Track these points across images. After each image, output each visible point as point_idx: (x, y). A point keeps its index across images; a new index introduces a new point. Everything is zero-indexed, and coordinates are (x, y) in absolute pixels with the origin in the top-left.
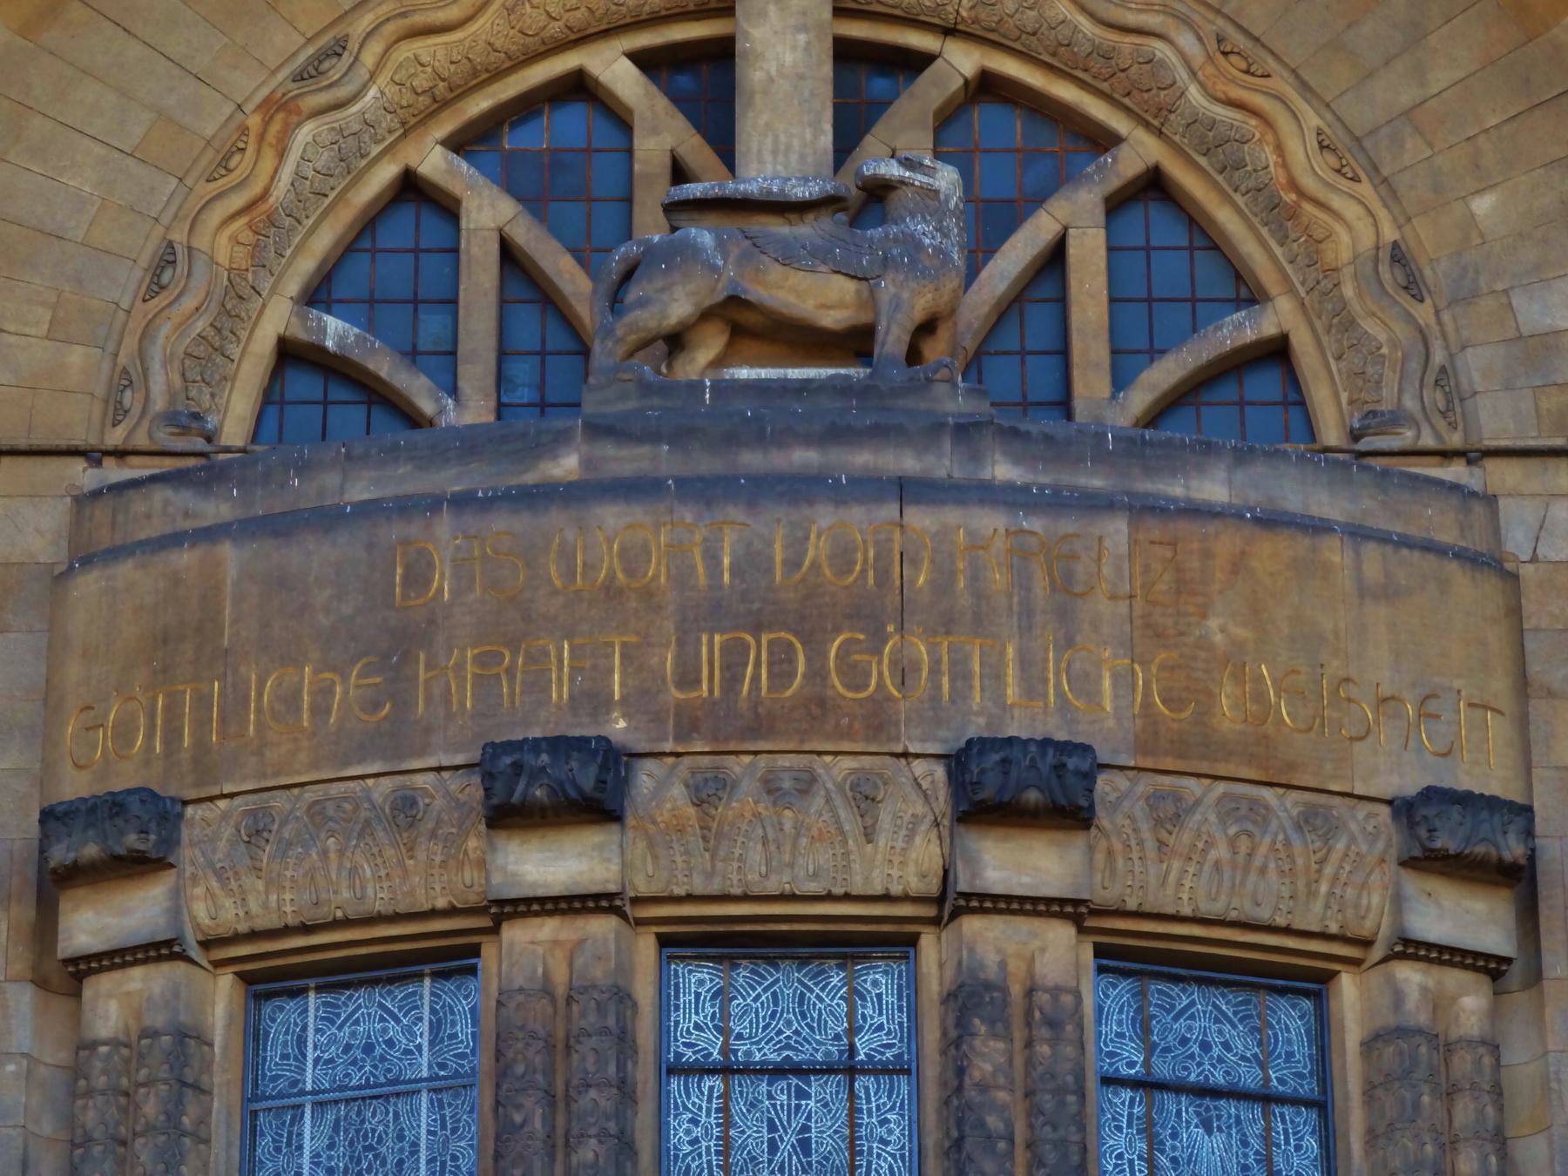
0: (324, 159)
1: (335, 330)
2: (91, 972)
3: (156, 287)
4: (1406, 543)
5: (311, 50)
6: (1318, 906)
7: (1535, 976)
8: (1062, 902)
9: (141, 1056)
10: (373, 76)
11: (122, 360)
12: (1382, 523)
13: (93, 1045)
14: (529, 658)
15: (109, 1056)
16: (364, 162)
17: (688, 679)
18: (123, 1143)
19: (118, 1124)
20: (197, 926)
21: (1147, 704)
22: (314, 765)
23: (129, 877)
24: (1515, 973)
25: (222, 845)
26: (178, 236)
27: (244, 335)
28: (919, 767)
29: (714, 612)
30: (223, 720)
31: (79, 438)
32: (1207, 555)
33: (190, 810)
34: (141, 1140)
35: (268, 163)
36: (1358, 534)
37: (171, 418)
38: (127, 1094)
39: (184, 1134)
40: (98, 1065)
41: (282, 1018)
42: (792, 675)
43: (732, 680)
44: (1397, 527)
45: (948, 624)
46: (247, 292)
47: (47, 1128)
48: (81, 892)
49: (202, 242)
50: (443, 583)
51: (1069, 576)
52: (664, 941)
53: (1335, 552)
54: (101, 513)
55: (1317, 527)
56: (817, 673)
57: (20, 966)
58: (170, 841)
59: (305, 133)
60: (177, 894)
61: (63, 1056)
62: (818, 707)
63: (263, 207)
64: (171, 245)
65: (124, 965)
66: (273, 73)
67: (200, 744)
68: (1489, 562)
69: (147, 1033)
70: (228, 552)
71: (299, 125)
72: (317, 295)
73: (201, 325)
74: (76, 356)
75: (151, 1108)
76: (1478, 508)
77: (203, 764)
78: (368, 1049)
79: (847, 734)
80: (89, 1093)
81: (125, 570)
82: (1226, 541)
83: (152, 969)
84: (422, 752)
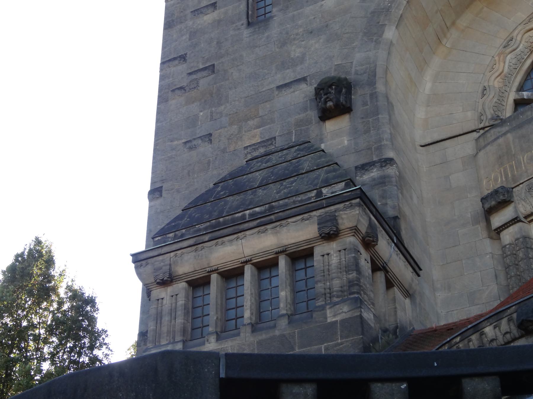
0: (514, 61)
1: (526, 95)
2: (501, 231)
3: (483, 95)
5: (506, 41)
9: (516, 245)
10: (520, 42)
11: (479, 111)
13: (505, 246)
15: (509, 248)
16: (523, 60)
18: (517, 265)
19: (515, 261)
20: (522, 214)
23: (504, 207)
25: (523, 195)
26: (486, 84)
27: (506, 100)
30: (517, 168)
31: (473, 128)
33: (514, 189)
34: (520, 262)
35: (502, 64)
37: (492, 119)
38: (515, 254)
39: (530, 258)
40: (507, 250)
46: (504, 91)
47: (500, 268)
48: (494, 215)
49: (491, 84)
54: (481, 140)
57: (485, 234)
58: (512, 196)
59: (509, 57)
60: (515, 207)
61: (500, 252)
63: (503, 74)
64: (485, 86)
65: (508, 227)
66: (499, 48)
67: (513, 175)
69: (517, 239)
70: (510, 136)
71: (507, 56)
72: (521, 88)
73: (495, 100)
74: (469, 114)
75: (521, 255)
77: (514, 179)
80: (507, 256)
81: (489, 147)
83: (514, 226)
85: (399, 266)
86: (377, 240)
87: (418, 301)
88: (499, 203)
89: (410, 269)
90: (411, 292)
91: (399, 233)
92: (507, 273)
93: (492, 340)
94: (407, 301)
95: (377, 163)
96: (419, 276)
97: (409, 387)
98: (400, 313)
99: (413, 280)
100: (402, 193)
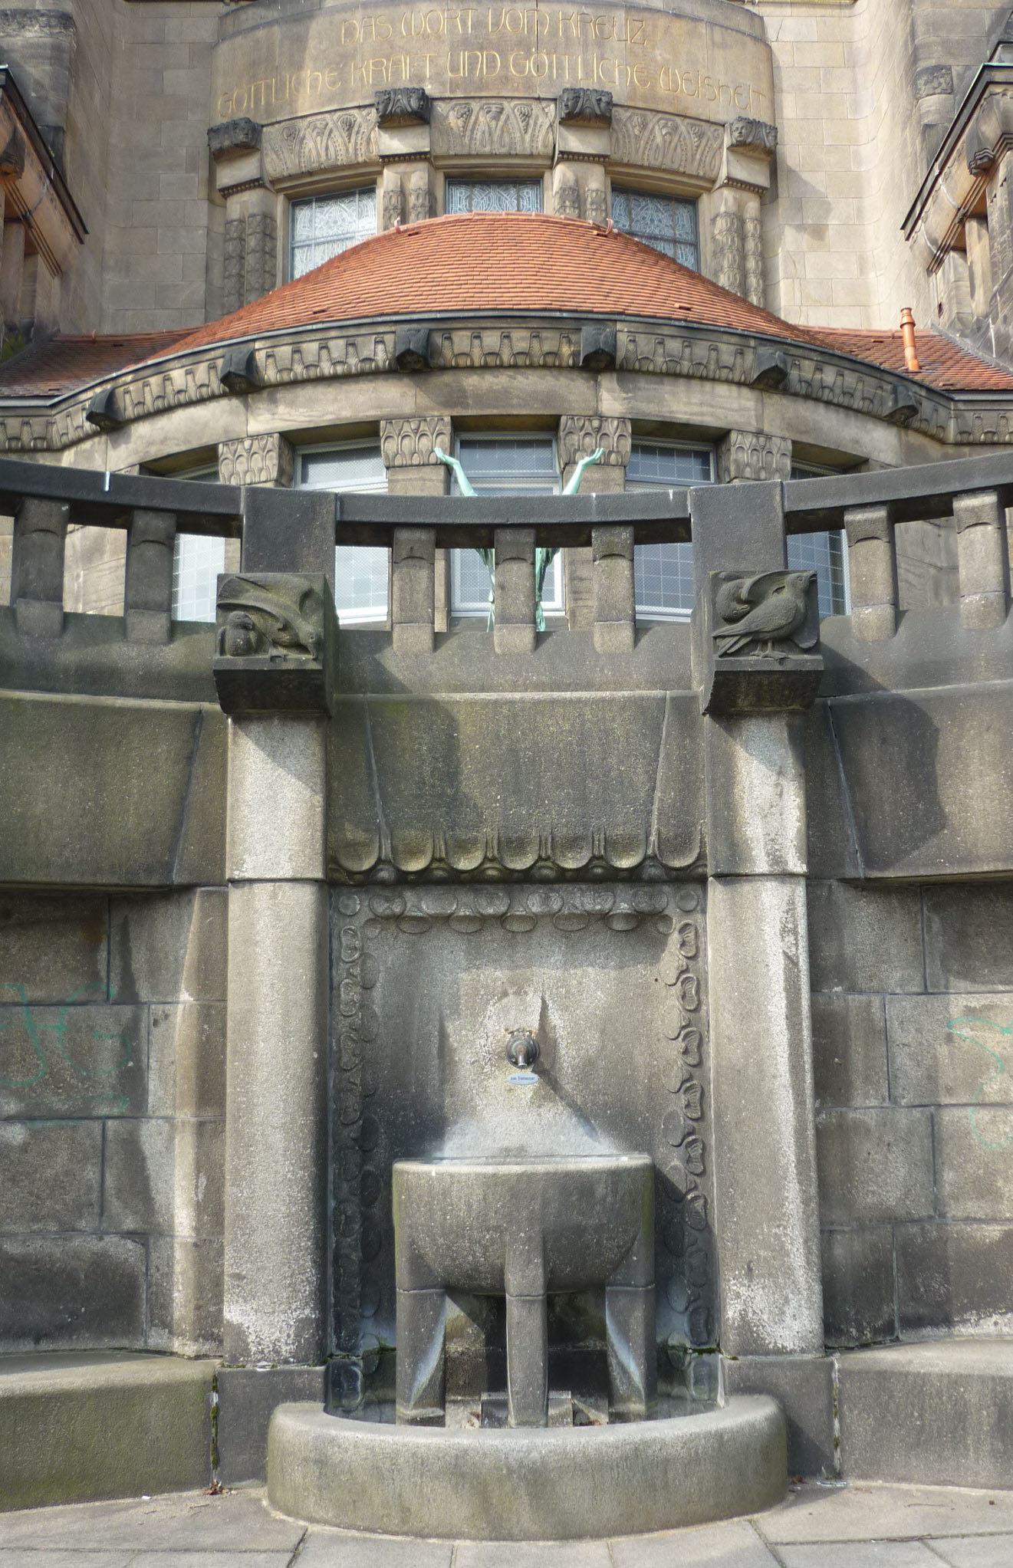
2: (230, 195)
4: (727, 28)
6: (696, 164)
7: (775, 197)
8: (599, 156)
12: (721, 20)
14: (394, 63)
17: (454, 69)
21: (632, 81)
22: (312, 108)
24: (768, 195)
28: (544, 104)
29: (466, 43)
32: (655, 26)
36: (712, 24)
41: (303, 215)
42: (495, 67)
43: (472, 70)
44: (727, 23)
45: (553, 49)
50: (359, 35)
51: (602, 31)
52: (447, 177)
53: (702, 28)
54: (229, 21)
55: (696, 20)
56: (505, 66)
57: (203, 193)
60: (261, 161)
62: (505, 79)
67: (268, 103)
68: (761, 40)
70: (276, 29)
76: (757, 20)
77: (269, 111)
78: (335, 222)
79: (517, 89)
80: (231, 239)
81: (239, 39)
82: (662, 22)
84: (353, 100)
85: (50, 219)
86: (22, 169)
87: (73, 283)
88: (237, 145)
89: (70, 228)
90: (64, 268)
91: (60, 157)
92: (225, 268)
93: (179, 392)
94: (56, 282)
95: (43, 15)
96: (82, 242)
97: (71, 510)
98: (40, 302)
99: (70, 249)
100: (76, 86)
